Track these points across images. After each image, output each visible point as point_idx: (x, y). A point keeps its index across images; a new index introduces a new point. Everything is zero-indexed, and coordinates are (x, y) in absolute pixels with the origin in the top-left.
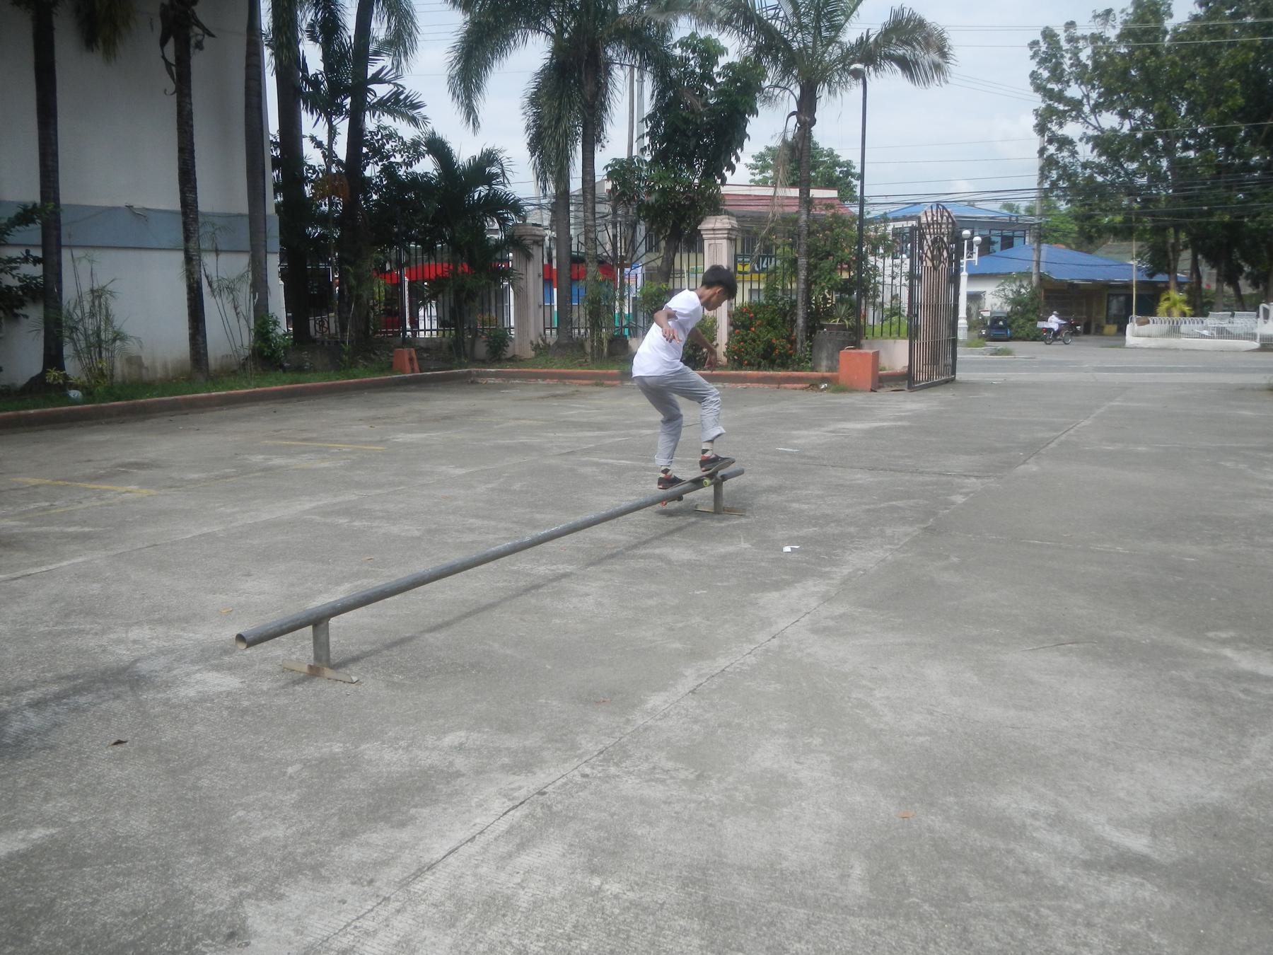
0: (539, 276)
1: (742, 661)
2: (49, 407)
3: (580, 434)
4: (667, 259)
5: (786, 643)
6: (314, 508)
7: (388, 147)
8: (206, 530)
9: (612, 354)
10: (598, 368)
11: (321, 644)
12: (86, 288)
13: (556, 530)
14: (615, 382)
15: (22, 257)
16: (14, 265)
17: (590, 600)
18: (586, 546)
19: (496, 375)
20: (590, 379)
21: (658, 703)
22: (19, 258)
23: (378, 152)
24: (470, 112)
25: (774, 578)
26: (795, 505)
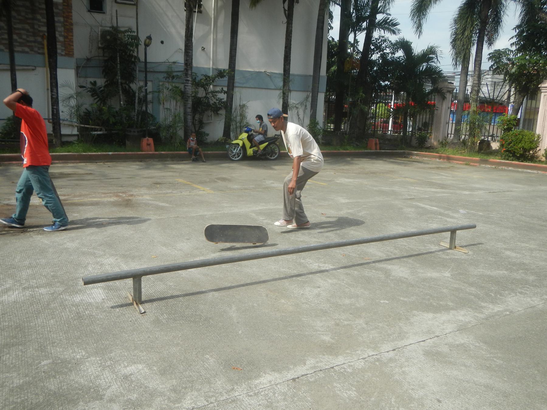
0: (449, 108)
1: (352, 364)
2: (122, 152)
3: (429, 189)
4: (519, 102)
5: (397, 357)
6: (260, 210)
7: (383, 45)
8: (206, 213)
9: (480, 149)
10: (469, 156)
11: (138, 290)
12: (238, 105)
13: (313, 246)
14: (476, 164)
15: (220, 90)
16: (215, 93)
17: (316, 291)
18: (355, 255)
19: (417, 155)
20: (463, 161)
21: (265, 381)
22: (219, 91)
23: (379, 48)
24: (419, 27)
25: (441, 303)
26: (508, 253)
